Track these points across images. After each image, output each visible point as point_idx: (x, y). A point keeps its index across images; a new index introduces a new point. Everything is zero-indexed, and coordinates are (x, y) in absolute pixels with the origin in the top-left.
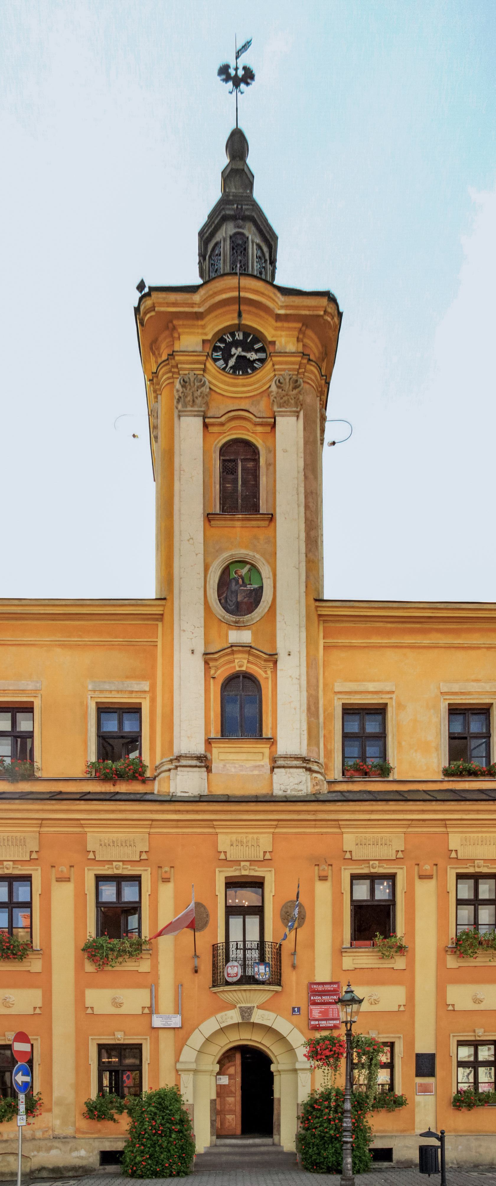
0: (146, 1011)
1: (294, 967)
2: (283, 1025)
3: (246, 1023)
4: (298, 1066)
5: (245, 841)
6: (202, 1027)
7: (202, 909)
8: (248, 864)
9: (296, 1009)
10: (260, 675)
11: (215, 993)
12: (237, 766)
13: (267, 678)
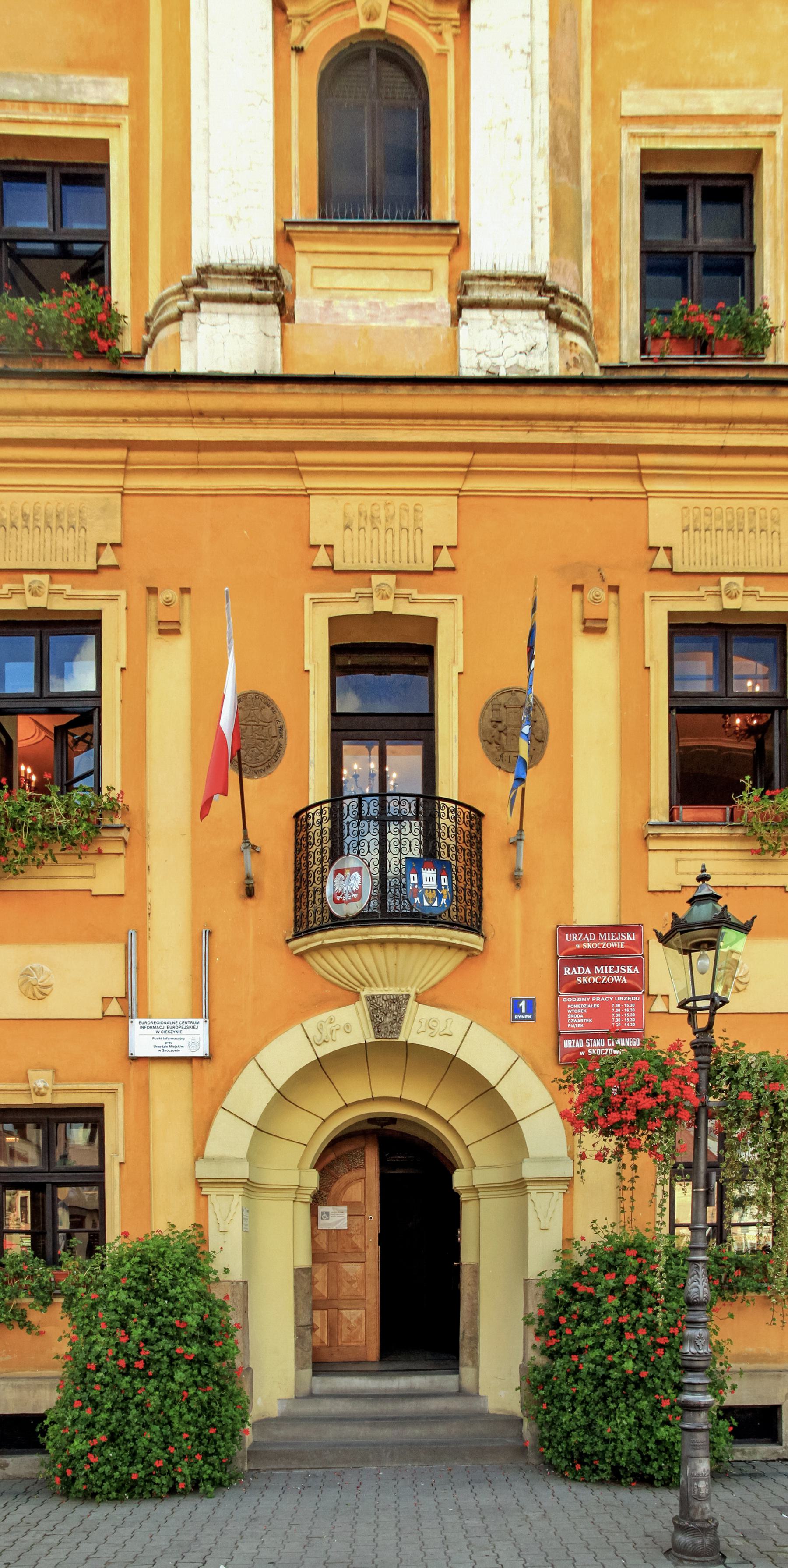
0: (114, 1009)
1: (516, 879)
2: (486, 1052)
3: (387, 1048)
4: (529, 1170)
5: (382, 514)
6: (266, 1056)
7: (267, 711)
8: (391, 579)
9: (523, 1004)
10: (427, 47)
11: (301, 955)
12: (362, 303)
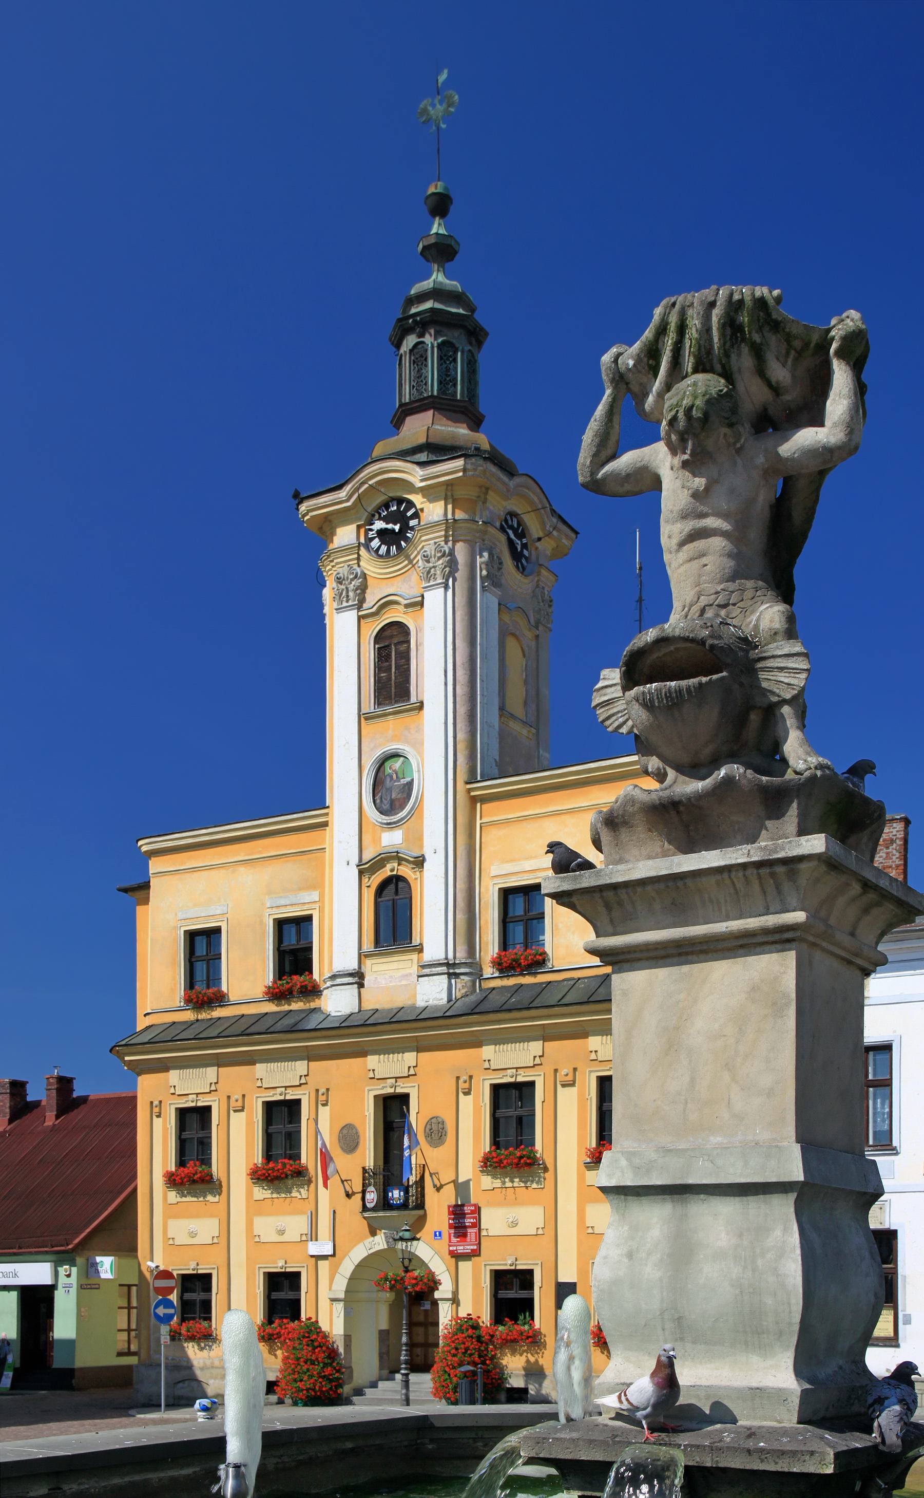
10: (410, 876)
13: (416, 879)
